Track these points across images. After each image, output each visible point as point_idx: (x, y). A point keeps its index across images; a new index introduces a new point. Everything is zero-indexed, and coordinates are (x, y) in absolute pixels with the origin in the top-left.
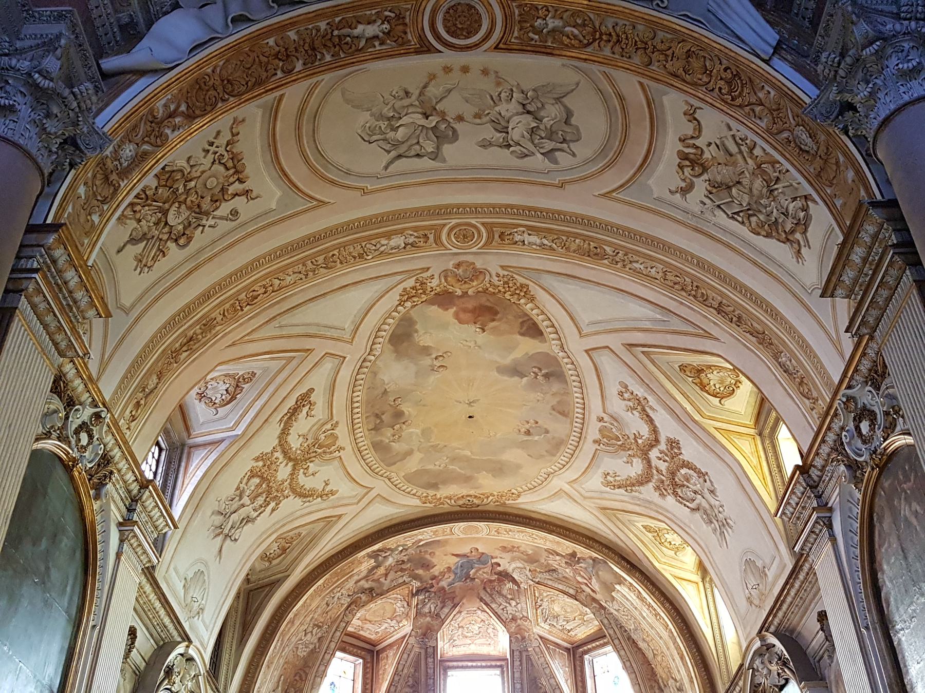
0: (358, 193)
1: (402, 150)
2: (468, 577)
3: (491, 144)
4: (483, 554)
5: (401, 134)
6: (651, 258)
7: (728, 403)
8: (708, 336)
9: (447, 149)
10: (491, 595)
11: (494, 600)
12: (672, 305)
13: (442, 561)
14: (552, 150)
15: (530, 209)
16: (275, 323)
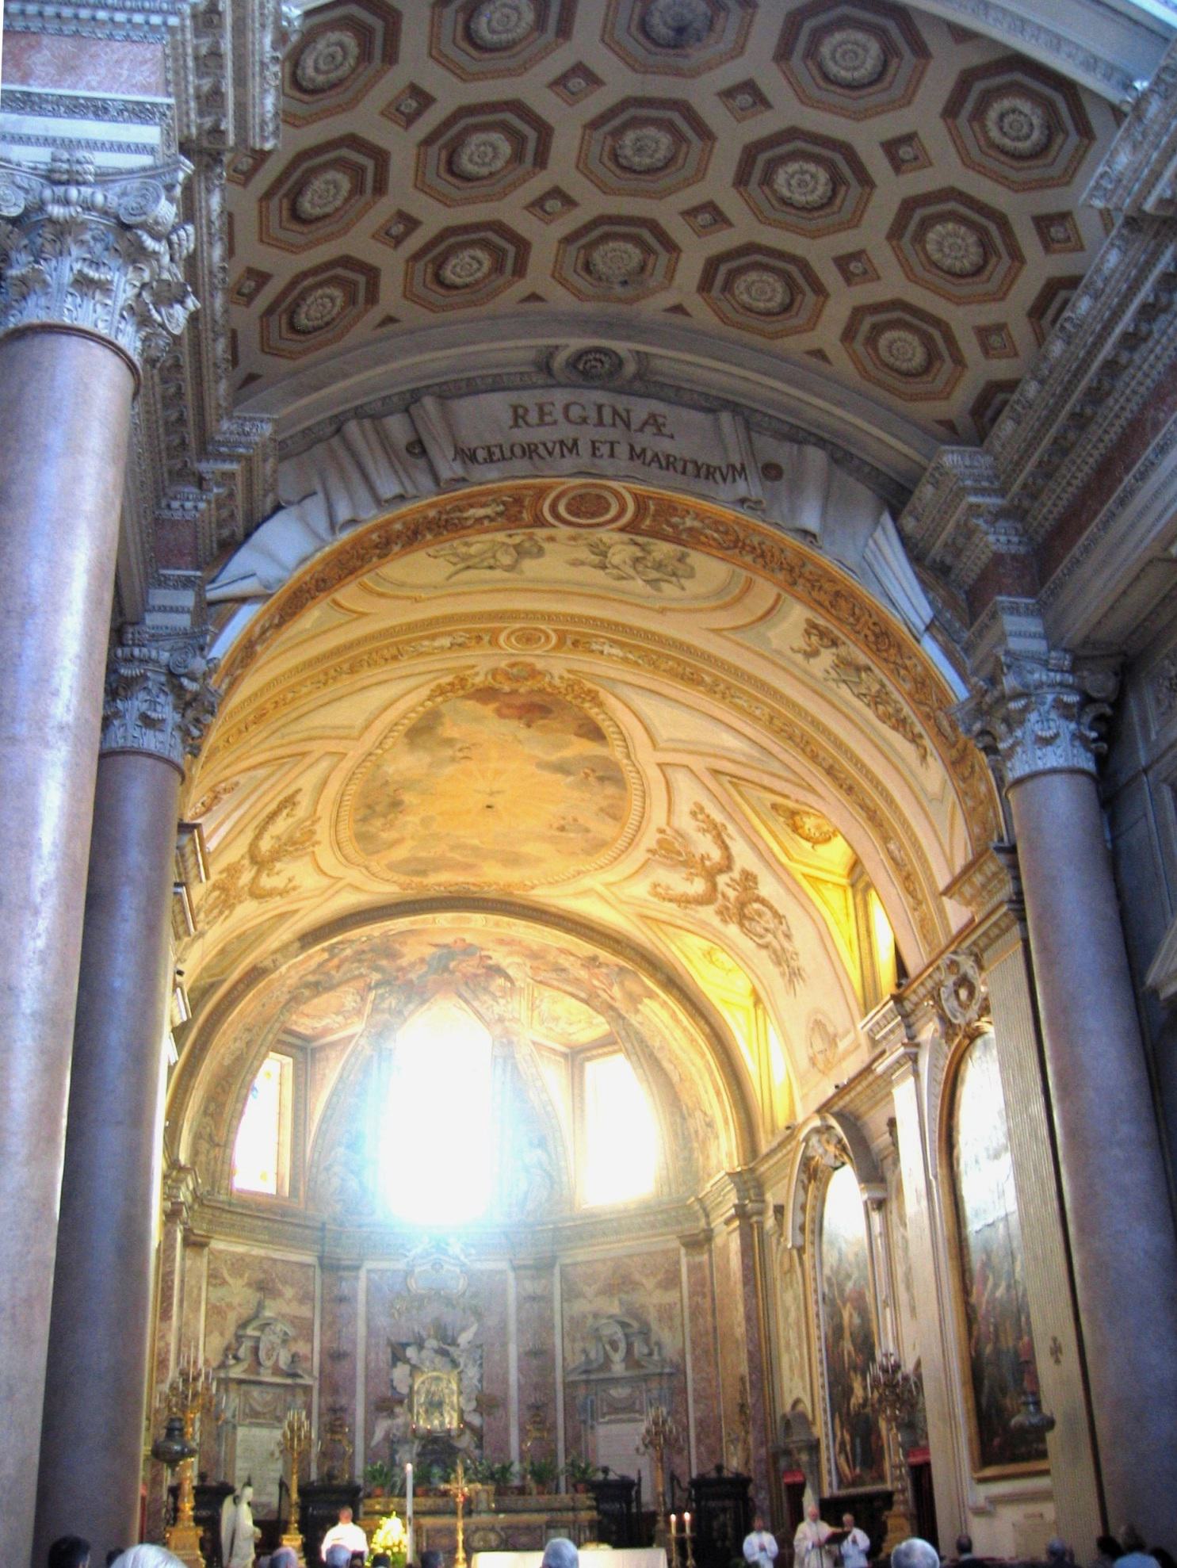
0: (409, 602)
1: (470, 563)
2: (446, 969)
3: (583, 563)
4: (471, 945)
5: (473, 550)
6: (757, 699)
7: (822, 849)
8: (813, 791)
9: (530, 566)
10: (473, 992)
11: (477, 998)
12: (775, 749)
13: (412, 952)
14: (657, 580)
15: (617, 624)
16: (279, 734)
